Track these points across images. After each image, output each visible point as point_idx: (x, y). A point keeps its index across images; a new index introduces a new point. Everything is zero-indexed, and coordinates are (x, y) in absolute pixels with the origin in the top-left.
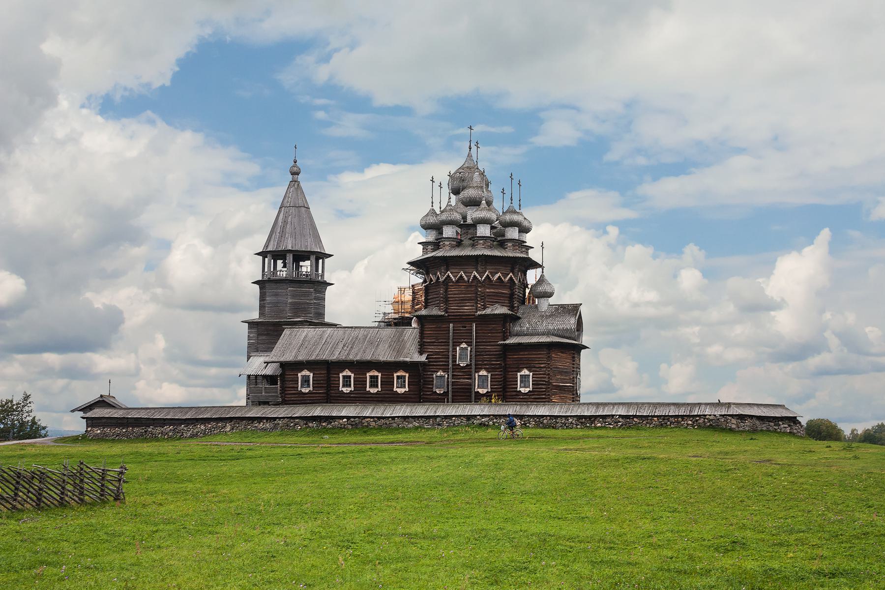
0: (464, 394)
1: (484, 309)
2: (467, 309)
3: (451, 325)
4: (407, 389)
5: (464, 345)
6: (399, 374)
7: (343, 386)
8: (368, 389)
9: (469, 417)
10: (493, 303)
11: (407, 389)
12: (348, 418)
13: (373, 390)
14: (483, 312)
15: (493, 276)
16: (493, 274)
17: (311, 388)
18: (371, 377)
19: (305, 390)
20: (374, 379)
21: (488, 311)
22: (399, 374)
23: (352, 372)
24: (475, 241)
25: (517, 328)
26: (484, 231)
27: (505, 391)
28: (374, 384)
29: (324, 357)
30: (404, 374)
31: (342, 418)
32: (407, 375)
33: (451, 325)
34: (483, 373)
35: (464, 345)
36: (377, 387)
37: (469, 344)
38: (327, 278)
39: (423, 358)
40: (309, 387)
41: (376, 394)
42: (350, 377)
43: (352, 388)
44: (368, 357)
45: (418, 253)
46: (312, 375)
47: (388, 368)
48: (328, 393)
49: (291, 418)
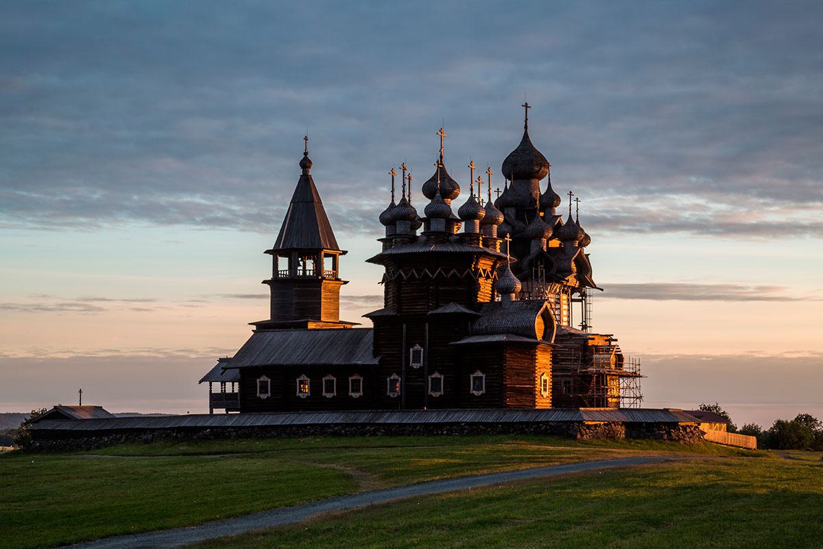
0: (414, 399)
1: (437, 307)
3: (404, 326)
4: (361, 393)
5: (417, 347)
9: (323, 426)
10: (447, 302)
11: (361, 393)
12: (211, 428)
13: (329, 396)
14: (435, 312)
15: (447, 273)
16: (447, 272)
19: (264, 396)
20: (330, 382)
21: (439, 311)
25: (476, 326)
27: (457, 398)
28: (329, 390)
29: (281, 362)
30: (358, 378)
31: (206, 428)
32: (362, 379)
33: (404, 326)
34: (436, 375)
35: (417, 347)
36: (333, 392)
37: (422, 345)
38: (342, 276)
39: (376, 362)
40: (440, 390)
45: (378, 249)
46: (269, 380)
47: (342, 371)
48: (285, 401)
49: (164, 429)
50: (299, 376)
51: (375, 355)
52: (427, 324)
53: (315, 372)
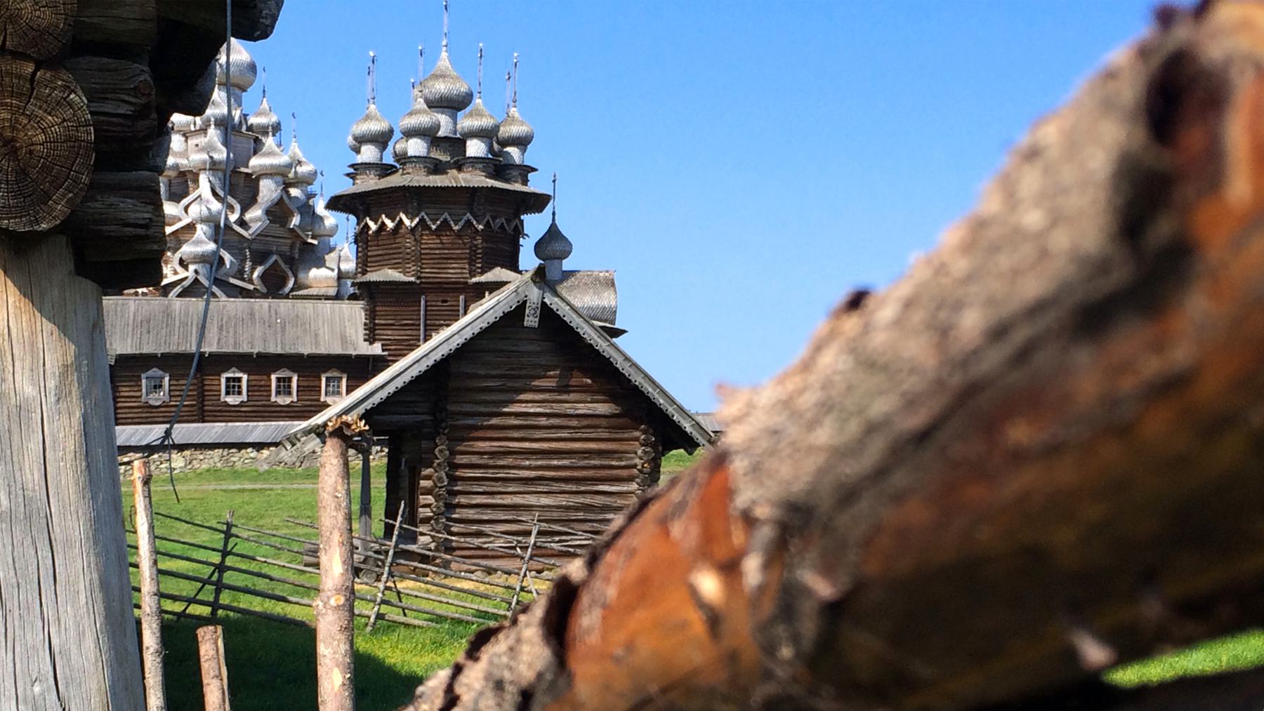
1: (482, 273)
2: (454, 272)
6: (329, 375)
7: (228, 393)
8: (273, 399)
16: (494, 218)
17: (167, 398)
18: (279, 380)
22: (329, 375)
23: (241, 371)
24: (461, 163)
26: (475, 148)
39: (377, 349)
41: (288, 406)
42: (239, 380)
43: (244, 397)
44: (274, 348)
50: (226, 370)
51: (371, 339)
52: (462, 297)
53: (260, 364)
